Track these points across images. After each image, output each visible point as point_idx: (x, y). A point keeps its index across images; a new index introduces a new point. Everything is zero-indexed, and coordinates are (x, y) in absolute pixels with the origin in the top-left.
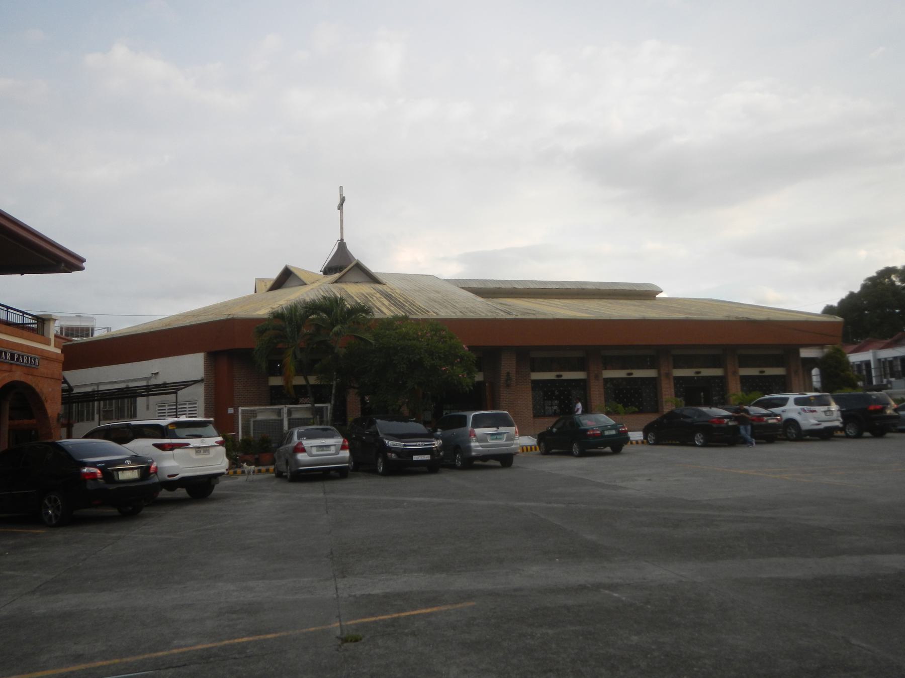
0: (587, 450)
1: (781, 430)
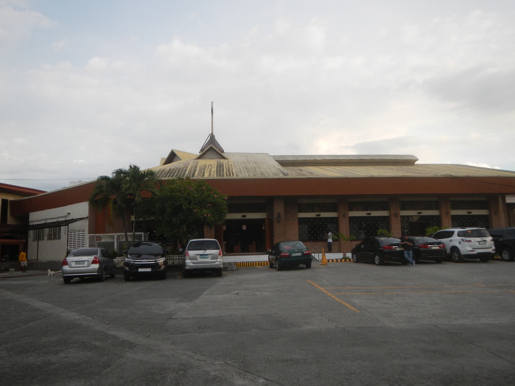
0: (385, 261)
1: (444, 254)
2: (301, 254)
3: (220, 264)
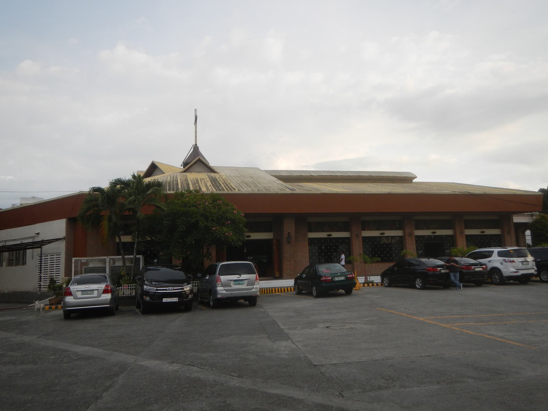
1: (486, 276)
2: (344, 278)
3: (256, 292)
